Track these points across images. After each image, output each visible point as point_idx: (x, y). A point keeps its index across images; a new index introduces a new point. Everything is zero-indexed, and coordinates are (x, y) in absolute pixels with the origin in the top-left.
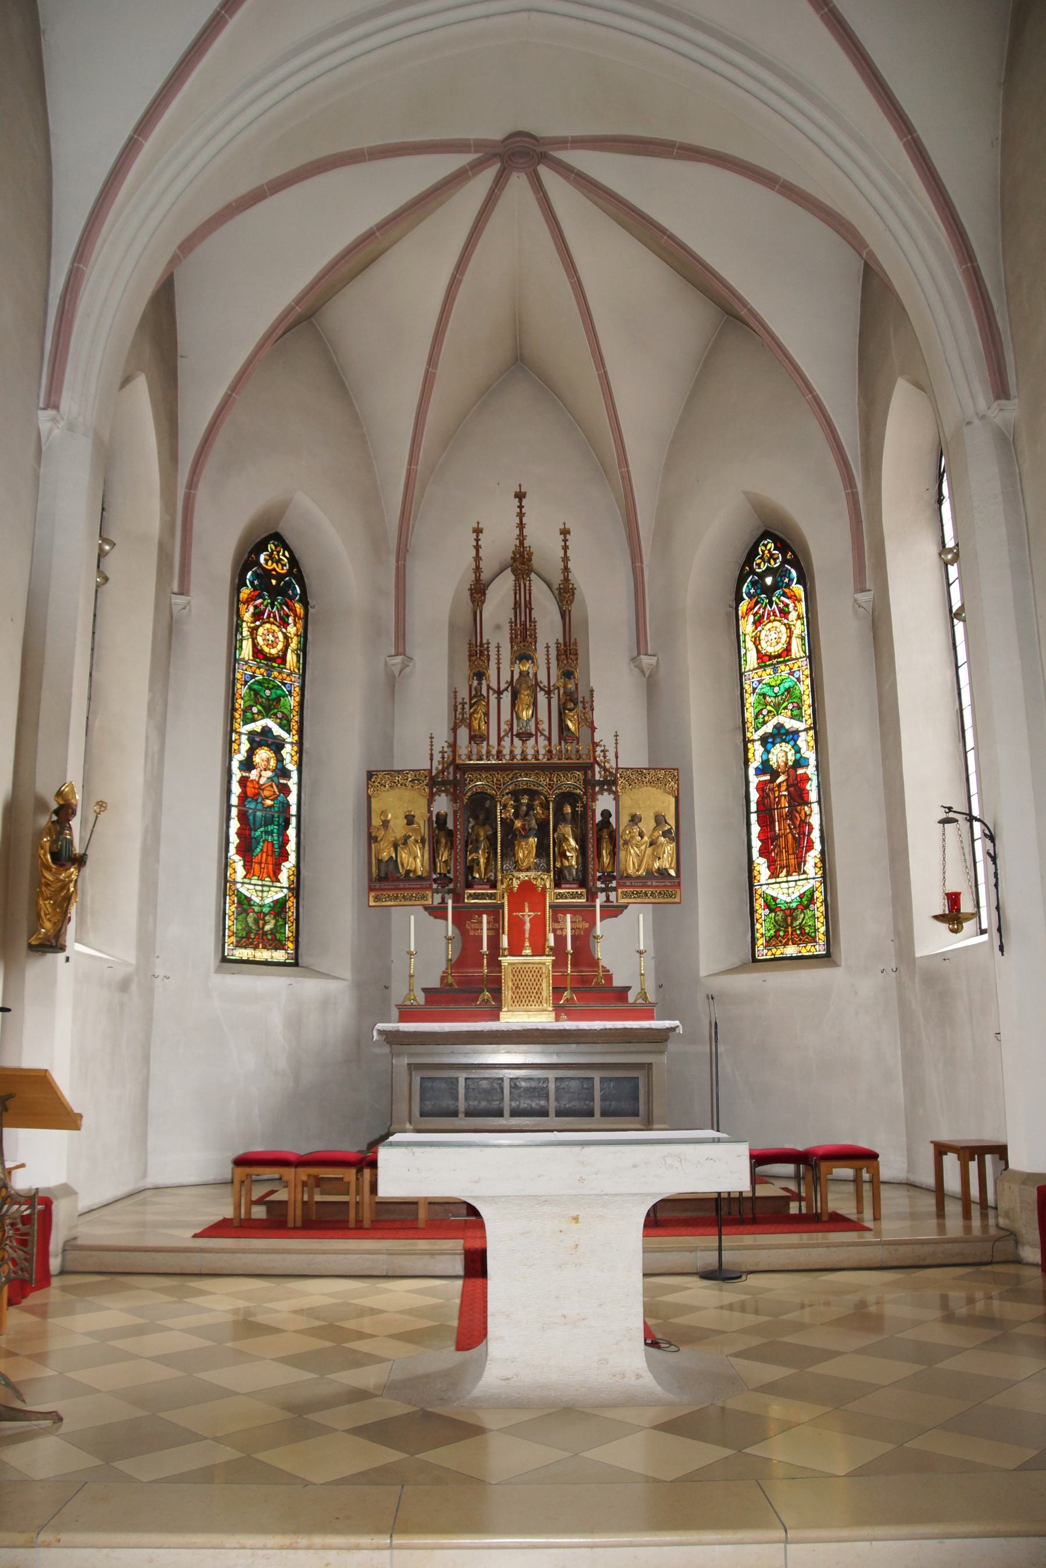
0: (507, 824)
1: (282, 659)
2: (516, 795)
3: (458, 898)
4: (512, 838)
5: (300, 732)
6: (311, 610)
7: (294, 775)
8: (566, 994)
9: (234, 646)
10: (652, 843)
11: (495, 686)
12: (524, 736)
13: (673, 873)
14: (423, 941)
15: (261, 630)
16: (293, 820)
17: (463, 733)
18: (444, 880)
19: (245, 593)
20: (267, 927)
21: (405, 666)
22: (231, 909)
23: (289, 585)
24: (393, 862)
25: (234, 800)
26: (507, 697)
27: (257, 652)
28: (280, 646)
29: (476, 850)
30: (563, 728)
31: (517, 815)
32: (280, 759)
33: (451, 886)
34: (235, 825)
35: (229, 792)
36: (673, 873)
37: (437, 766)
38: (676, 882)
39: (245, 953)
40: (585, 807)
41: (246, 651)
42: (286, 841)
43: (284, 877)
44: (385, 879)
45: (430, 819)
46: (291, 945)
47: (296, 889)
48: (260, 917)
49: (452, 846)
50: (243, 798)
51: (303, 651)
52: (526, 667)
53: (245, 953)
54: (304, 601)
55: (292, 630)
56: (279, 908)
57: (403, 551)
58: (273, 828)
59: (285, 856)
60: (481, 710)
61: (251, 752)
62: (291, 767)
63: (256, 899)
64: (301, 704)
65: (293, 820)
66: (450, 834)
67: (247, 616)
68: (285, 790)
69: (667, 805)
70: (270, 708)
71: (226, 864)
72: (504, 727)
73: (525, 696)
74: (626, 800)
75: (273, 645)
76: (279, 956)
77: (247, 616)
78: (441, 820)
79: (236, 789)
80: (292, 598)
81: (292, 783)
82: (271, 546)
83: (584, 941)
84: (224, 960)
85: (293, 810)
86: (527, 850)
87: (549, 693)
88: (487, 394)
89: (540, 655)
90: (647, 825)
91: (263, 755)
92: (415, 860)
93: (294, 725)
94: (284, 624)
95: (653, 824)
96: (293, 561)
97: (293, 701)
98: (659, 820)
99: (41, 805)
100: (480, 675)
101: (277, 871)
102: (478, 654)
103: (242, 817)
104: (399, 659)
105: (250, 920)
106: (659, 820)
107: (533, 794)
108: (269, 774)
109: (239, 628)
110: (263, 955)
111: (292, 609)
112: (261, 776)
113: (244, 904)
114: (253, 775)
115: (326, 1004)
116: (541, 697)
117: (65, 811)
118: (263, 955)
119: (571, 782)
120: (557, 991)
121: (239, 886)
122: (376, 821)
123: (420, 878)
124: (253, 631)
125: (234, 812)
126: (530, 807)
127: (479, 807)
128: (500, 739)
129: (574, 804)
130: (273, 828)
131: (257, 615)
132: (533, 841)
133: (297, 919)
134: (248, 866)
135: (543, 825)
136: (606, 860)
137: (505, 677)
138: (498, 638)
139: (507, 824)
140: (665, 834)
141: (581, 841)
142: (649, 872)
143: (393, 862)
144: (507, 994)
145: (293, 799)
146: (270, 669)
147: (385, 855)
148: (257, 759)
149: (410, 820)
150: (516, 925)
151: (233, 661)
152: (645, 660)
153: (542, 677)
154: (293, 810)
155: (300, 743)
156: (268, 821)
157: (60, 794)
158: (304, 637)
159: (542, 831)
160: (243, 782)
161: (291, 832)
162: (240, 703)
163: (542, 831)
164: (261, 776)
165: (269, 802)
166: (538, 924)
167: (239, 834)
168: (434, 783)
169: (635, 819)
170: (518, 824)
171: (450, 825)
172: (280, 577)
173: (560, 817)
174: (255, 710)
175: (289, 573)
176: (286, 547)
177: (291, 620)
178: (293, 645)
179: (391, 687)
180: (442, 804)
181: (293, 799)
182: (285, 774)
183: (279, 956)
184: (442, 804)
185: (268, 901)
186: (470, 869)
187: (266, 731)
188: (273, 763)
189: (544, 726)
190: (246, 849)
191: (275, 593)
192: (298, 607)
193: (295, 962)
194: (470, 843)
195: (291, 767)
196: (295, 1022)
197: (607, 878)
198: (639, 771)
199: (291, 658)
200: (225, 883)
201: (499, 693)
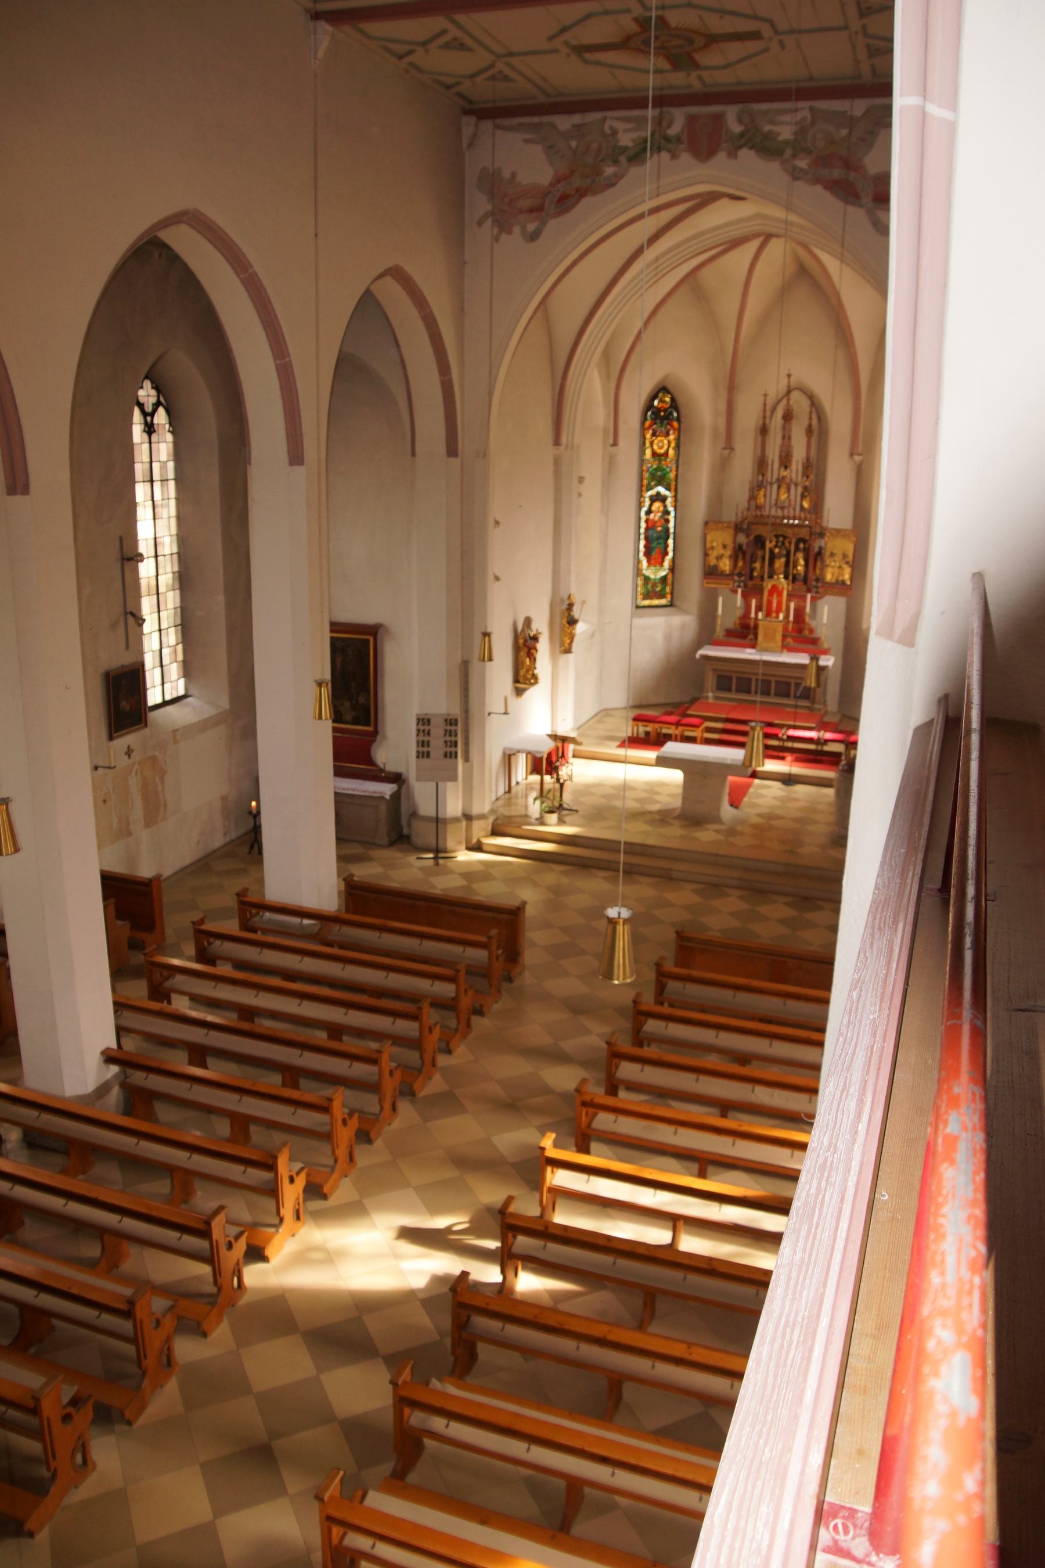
0: (771, 551)
1: (666, 454)
2: (777, 536)
3: (745, 586)
4: (773, 557)
5: (676, 490)
6: (683, 425)
7: (673, 514)
8: (789, 640)
9: (642, 452)
10: (840, 567)
11: (769, 480)
12: (783, 508)
13: (848, 583)
14: (730, 605)
15: (656, 442)
16: (672, 536)
17: (753, 503)
18: (740, 575)
19: (647, 423)
20: (658, 589)
21: (729, 454)
22: (640, 582)
23: (671, 414)
24: (716, 567)
25: (642, 531)
26: (775, 487)
27: (654, 454)
28: (666, 447)
29: (755, 562)
30: (802, 507)
31: (776, 546)
32: (665, 506)
33: (743, 578)
34: (642, 543)
35: (639, 527)
36: (848, 583)
37: (739, 519)
38: (850, 588)
39: (647, 602)
40: (810, 546)
41: (648, 453)
42: (667, 546)
43: (667, 564)
44: (711, 573)
45: (734, 547)
46: (669, 596)
47: (672, 569)
48: (654, 585)
49: (744, 559)
50: (647, 529)
51: (678, 447)
52: (784, 473)
53: (647, 602)
54: (678, 419)
55: (672, 437)
56: (664, 579)
57: (732, 389)
58: (662, 541)
59: (666, 554)
60: (762, 493)
61: (651, 506)
62: (671, 509)
63: (652, 577)
64: (676, 476)
65: (672, 536)
66: (744, 553)
67: (648, 436)
68: (667, 521)
69: (850, 548)
70: (659, 484)
71: (639, 562)
72: (773, 502)
73: (783, 490)
74: (830, 545)
75: (661, 448)
76: (663, 602)
77: (648, 436)
78: (740, 547)
79: (643, 525)
80: (672, 420)
81: (671, 518)
82: (660, 395)
83: (799, 614)
84: (637, 607)
85: (672, 530)
86: (780, 563)
87: (796, 485)
88: (784, 293)
89: (794, 467)
90: (838, 557)
91: (657, 505)
92: (726, 565)
93: (673, 487)
94: (667, 435)
95: (841, 557)
96: (673, 399)
97: (672, 475)
98: (845, 556)
99: (562, 601)
100: (763, 475)
101: (663, 561)
102: (761, 464)
103: (646, 538)
104: (726, 452)
105: (649, 586)
106: (845, 556)
107: (785, 537)
108: (660, 514)
109: (644, 444)
110: (656, 602)
111: (672, 426)
112: (655, 517)
113: (647, 579)
114: (652, 516)
115: (683, 627)
116: (793, 487)
117: (570, 606)
118: (656, 602)
119: (804, 533)
120: (784, 637)
121: (644, 572)
122: (708, 545)
123: (728, 575)
124: (652, 443)
125: (642, 537)
126: (783, 543)
127: (760, 541)
128: (770, 508)
129: (804, 544)
130: (662, 541)
131: (654, 434)
132: (783, 560)
133: (673, 584)
134: (649, 561)
135: (788, 552)
136: (818, 572)
137: (775, 477)
138: (773, 453)
139: (771, 551)
140: (847, 563)
141: (806, 560)
142: (837, 581)
143: (716, 567)
144: (760, 637)
145: (671, 525)
146: (660, 461)
147: (712, 564)
148: (654, 508)
149: (724, 547)
150: (770, 603)
151: (642, 461)
152: (857, 458)
153: (794, 477)
154: (672, 530)
155: (675, 496)
156: (659, 538)
157: (569, 597)
158: (678, 440)
159: (788, 556)
160: (647, 521)
161: (671, 542)
162: (645, 482)
163: (788, 556)
164: (655, 517)
165: (659, 529)
166: (779, 603)
167: (645, 546)
168: (738, 528)
169: (832, 555)
170: (777, 550)
171: (744, 548)
172: (665, 410)
173: (797, 549)
174: (653, 483)
175: (671, 407)
176: (668, 392)
177: (671, 432)
178: (673, 445)
179: (723, 465)
180: (742, 538)
181: (671, 525)
182: (668, 513)
183: (663, 602)
184: (742, 538)
185: (658, 577)
186: (752, 570)
187: (658, 493)
188: (662, 509)
189: (793, 503)
190: (647, 554)
191: (663, 419)
192: (675, 424)
193: (671, 605)
194: (753, 561)
195: (671, 509)
196: (668, 637)
197: (817, 580)
198: (838, 531)
199: (671, 452)
200: (638, 571)
201: (771, 484)
